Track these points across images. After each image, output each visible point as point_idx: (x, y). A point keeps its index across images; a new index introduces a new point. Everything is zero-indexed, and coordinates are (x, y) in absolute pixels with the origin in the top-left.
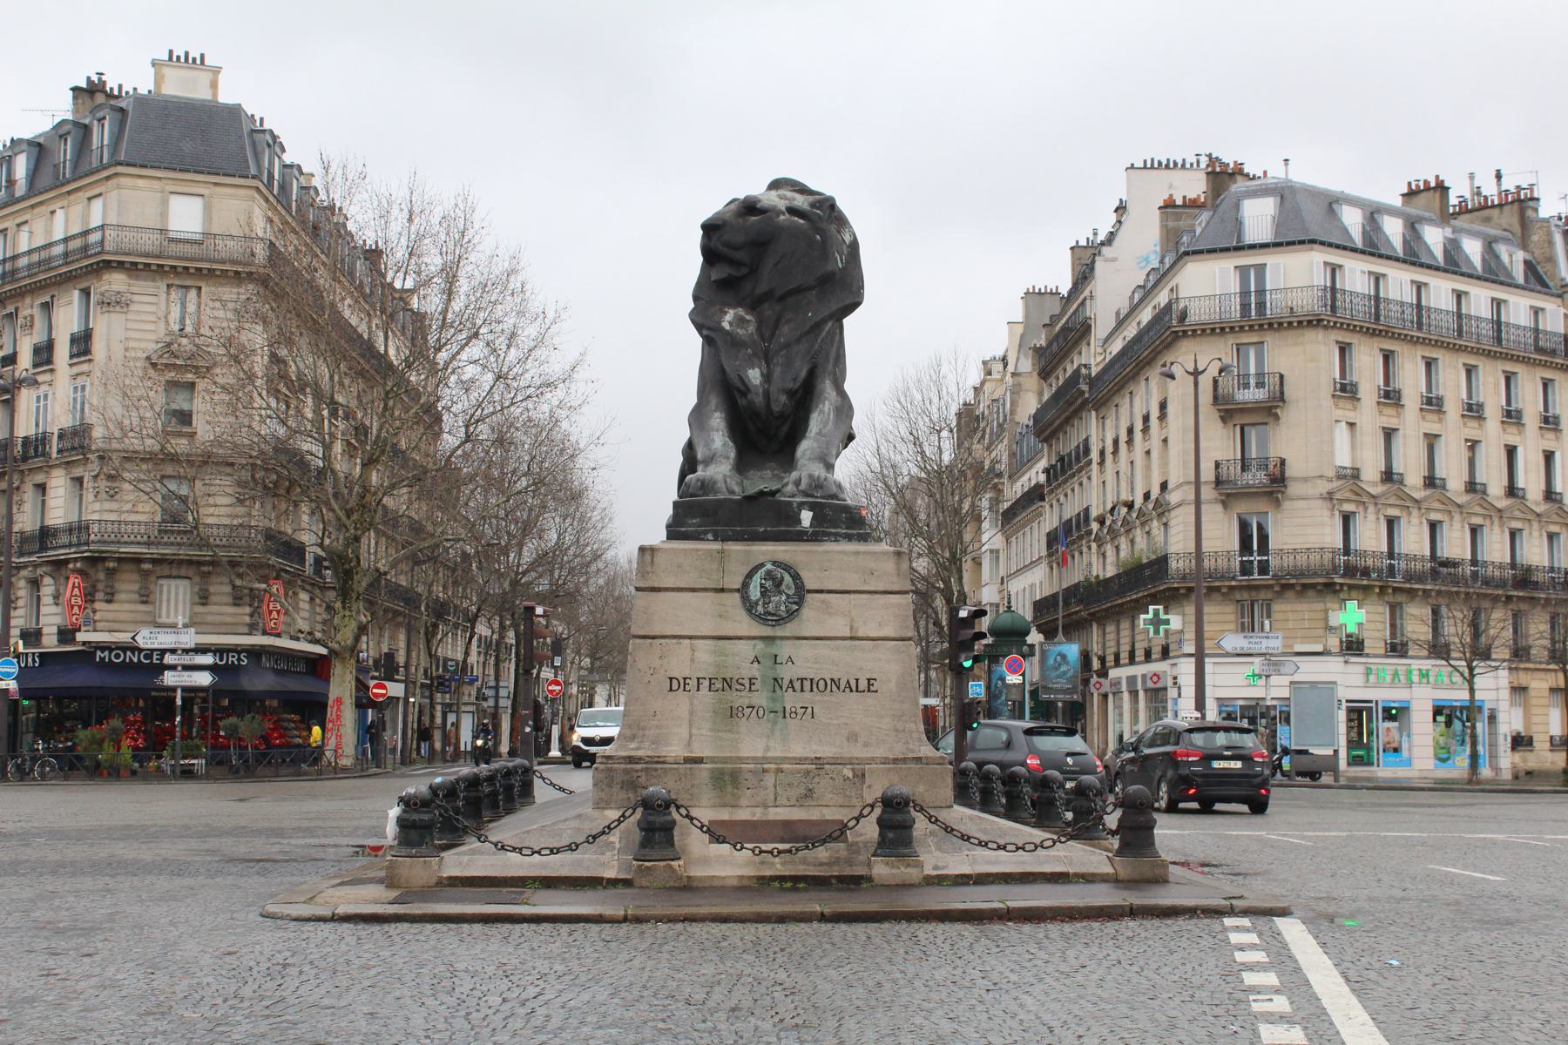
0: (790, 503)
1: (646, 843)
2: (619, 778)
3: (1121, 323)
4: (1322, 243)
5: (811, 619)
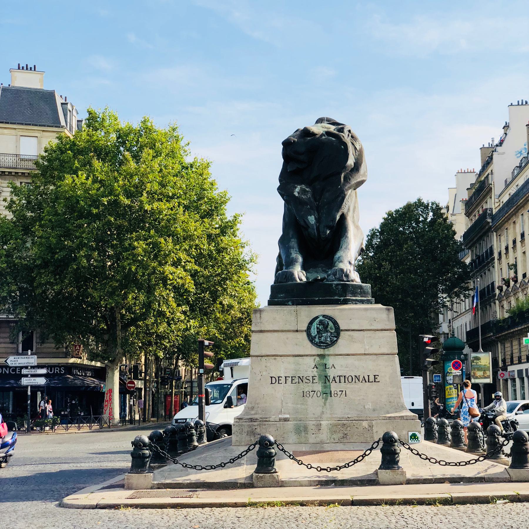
0: (332, 285)
2: (246, 429)
3: (507, 185)
5: (343, 345)
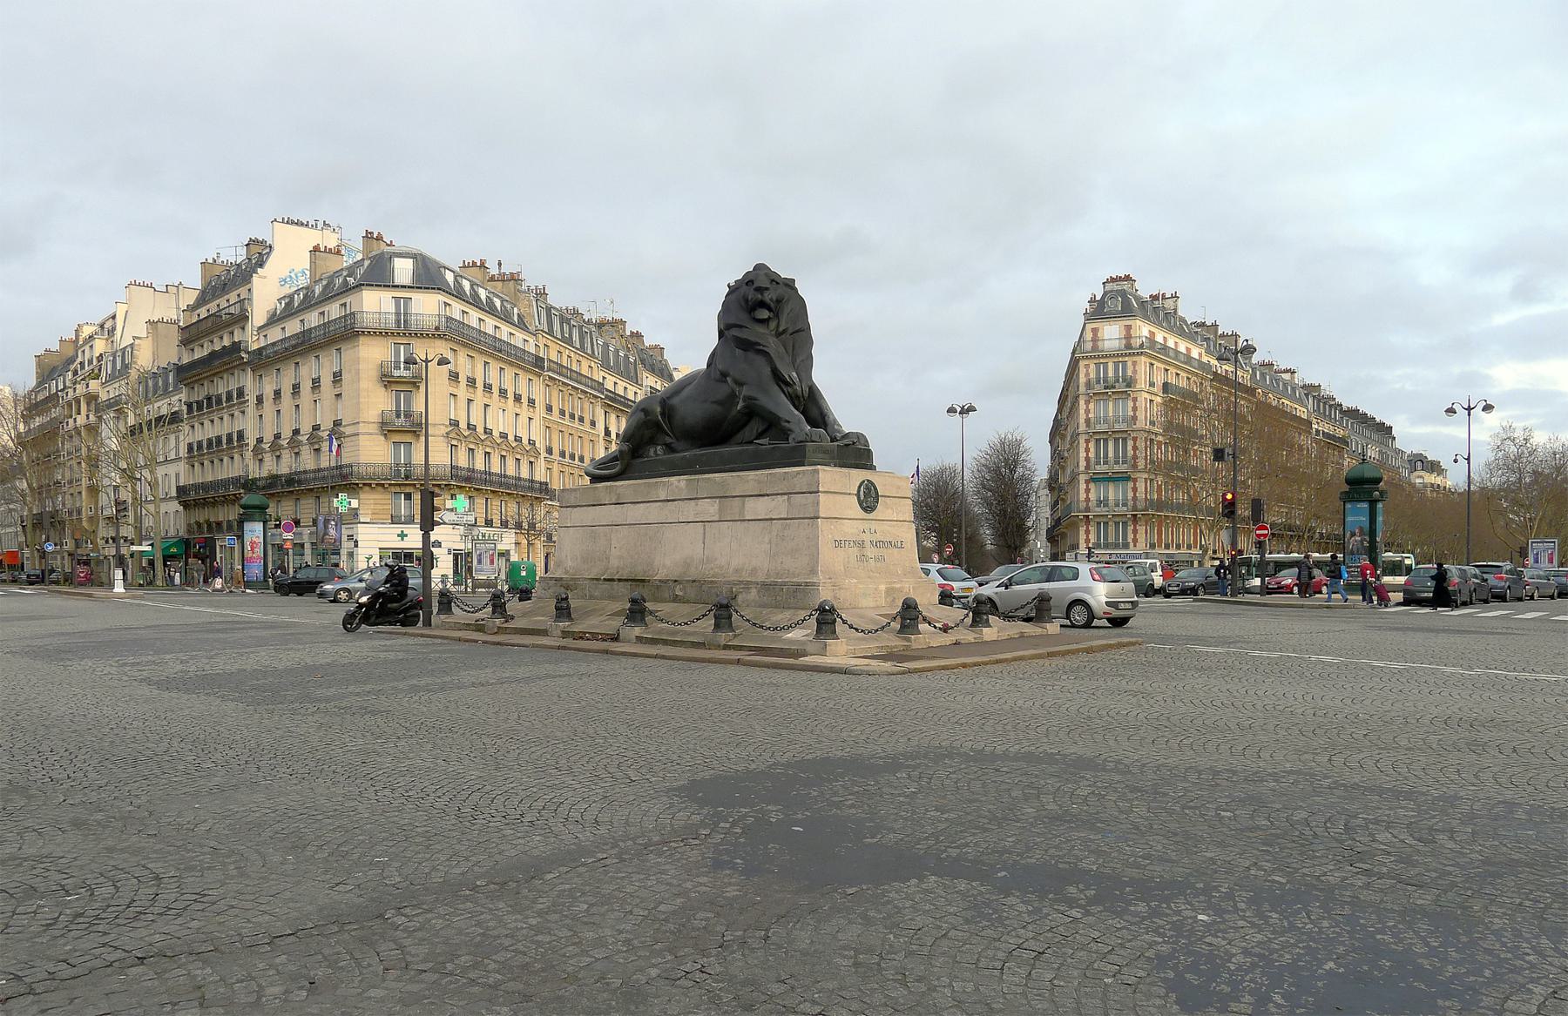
1: (819, 630)
3: (274, 320)
5: (881, 511)
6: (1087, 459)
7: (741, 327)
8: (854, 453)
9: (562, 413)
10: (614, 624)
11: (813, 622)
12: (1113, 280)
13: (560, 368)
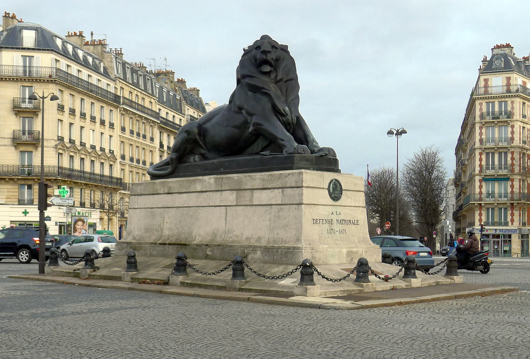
4: (55, 52)
5: (344, 200)
6: (481, 166)
7: (251, 77)
8: (326, 161)
9: (132, 132)
10: (164, 274)
11: (298, 273)
12: (498, 47)
13: (131, 103)
